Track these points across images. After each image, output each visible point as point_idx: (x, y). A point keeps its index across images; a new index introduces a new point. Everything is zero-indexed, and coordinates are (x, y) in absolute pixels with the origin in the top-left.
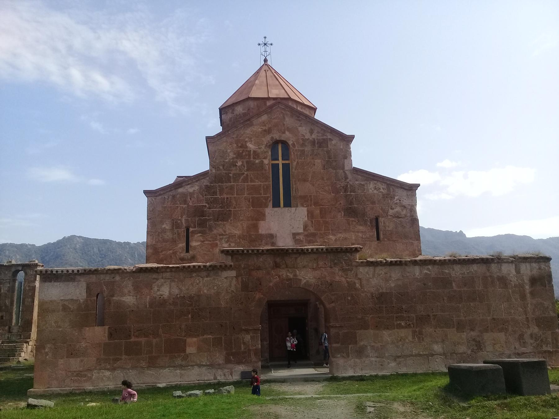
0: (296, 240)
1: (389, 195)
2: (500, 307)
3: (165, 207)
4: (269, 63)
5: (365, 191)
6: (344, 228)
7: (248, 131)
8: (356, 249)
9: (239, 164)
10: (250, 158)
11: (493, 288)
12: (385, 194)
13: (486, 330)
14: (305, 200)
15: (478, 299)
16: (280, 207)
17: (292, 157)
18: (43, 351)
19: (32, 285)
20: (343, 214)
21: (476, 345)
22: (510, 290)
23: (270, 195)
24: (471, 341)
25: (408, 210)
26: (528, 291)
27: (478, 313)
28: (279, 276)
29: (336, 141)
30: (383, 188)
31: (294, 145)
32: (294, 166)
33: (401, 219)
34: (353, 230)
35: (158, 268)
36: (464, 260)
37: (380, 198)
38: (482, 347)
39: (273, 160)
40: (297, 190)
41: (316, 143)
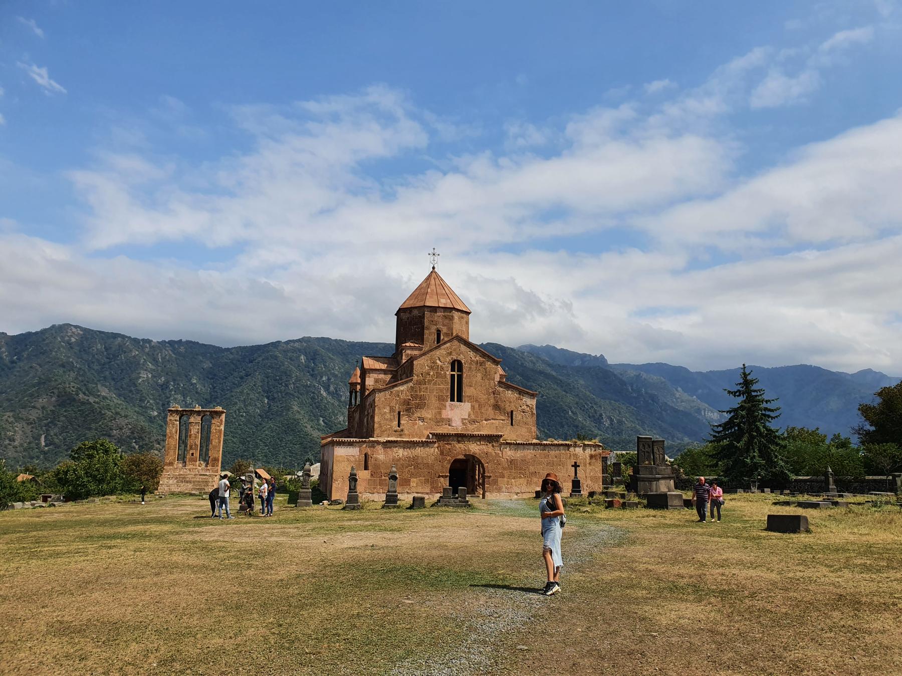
3: (386, 399)
4: (436, 270)
6: (492, 417)
7: (438, 353)
8: (501, 436)
9: (431, 374)
10: (438, 370)
13: (565, 481)
14: (471, 399)
16: (454, 401)
17: (464, 370)
18: (337, 482)
19: (218, 428)
23: (449, 394)
28: (460, 448)
35: (397, 441)
36: (556, 444)
39: (451, 371)
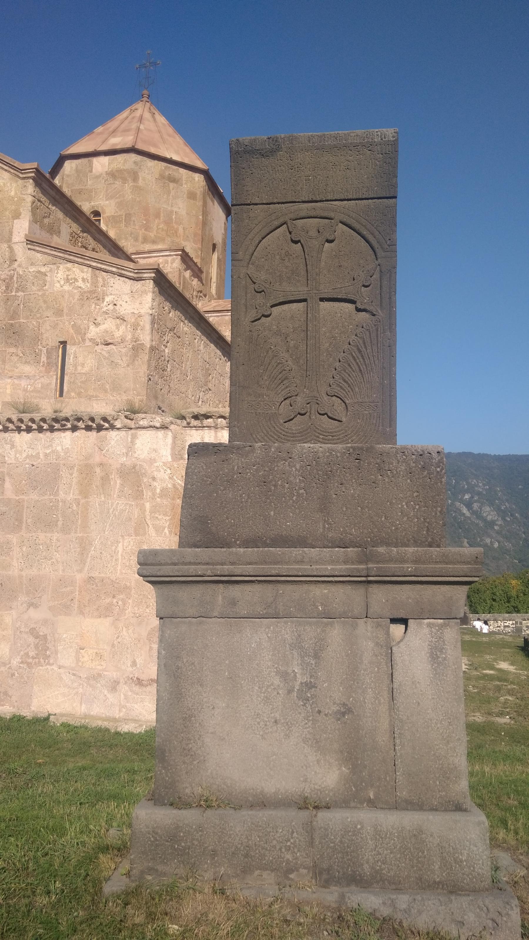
1: (94, 293)
2: (114, 548)
5: (46, 287)
11: (102, 496)
12: (85, 292)
15: (60, 523)
21: (36, 646)
22: (148, 505)
24: (27, 633)
25: (129, 326)
27: (54, 560)
29: (3, 181)
30: (83, 280)
33: (114, 347)
34: (10, 374)
37: (73, 302)
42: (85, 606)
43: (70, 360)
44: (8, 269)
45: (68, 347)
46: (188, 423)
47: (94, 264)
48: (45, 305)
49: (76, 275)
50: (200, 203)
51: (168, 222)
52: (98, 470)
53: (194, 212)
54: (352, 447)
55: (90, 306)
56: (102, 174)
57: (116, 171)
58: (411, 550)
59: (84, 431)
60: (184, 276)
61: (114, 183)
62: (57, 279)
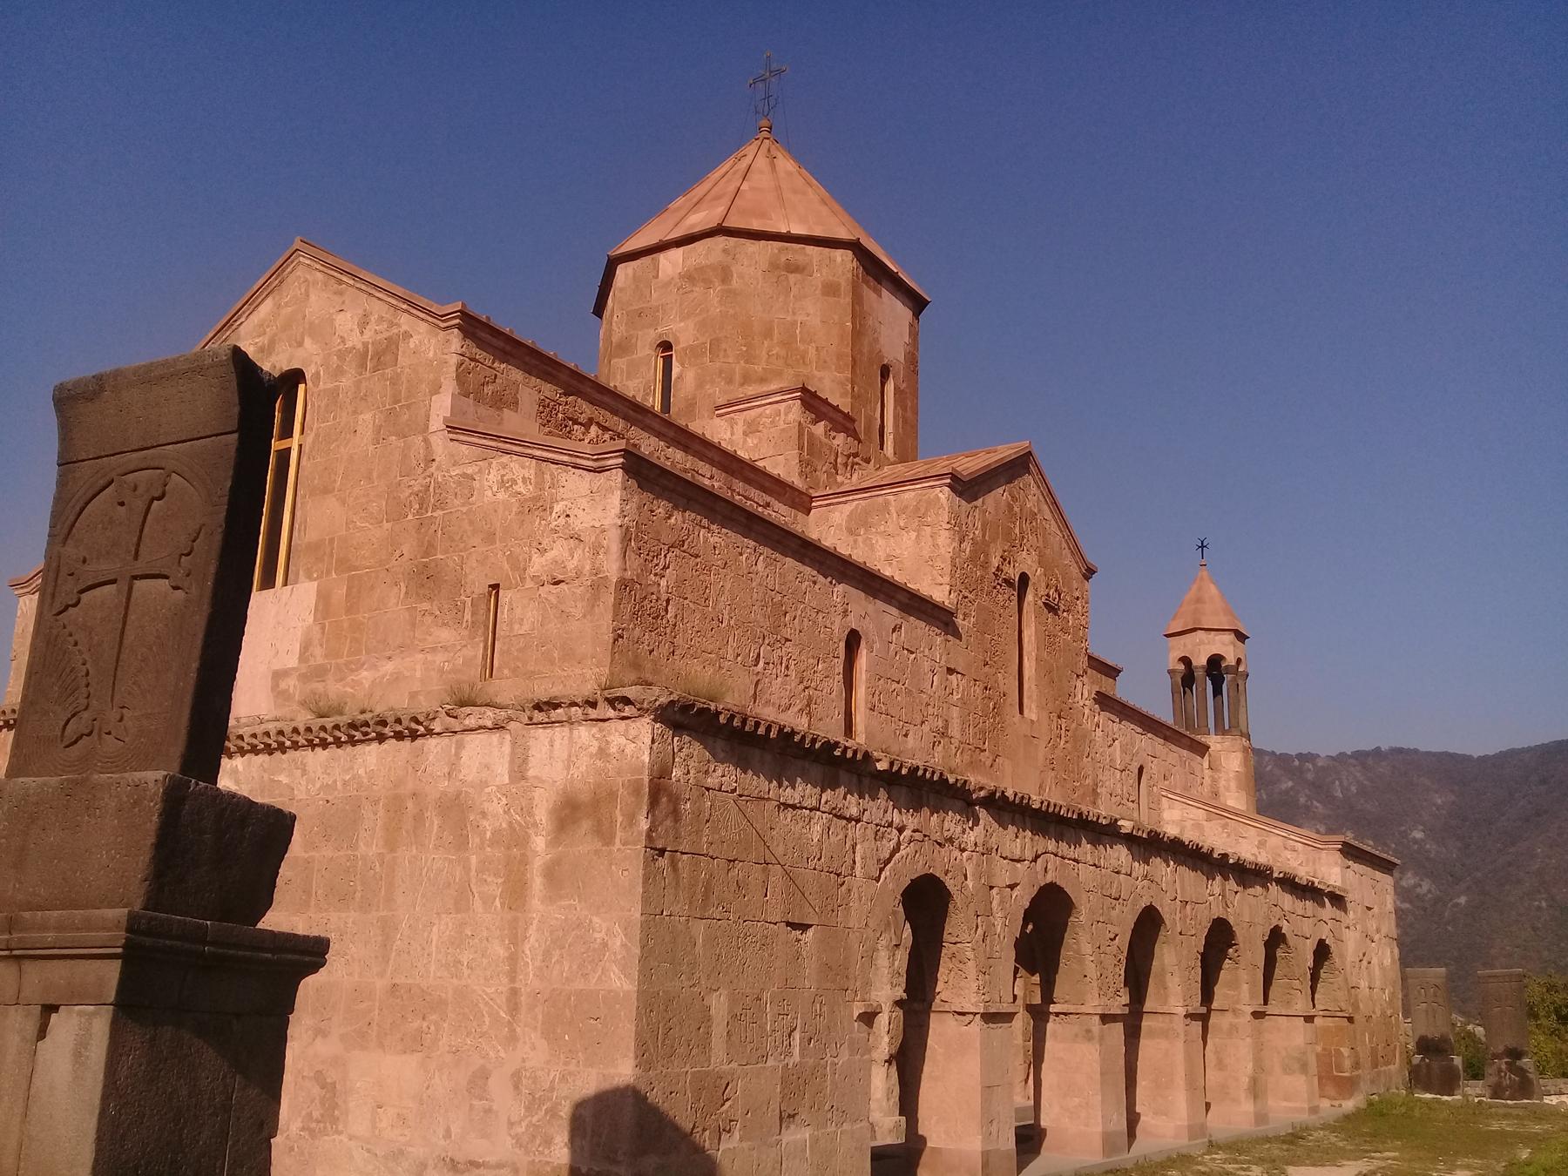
0: (279, 693)
2: (426, 934)
5: (474, 498)
12: (526, 500)
15: (358, 895)
20: (403, 589)
22: (474, 859)
25: (587, 549)
26: (537, 864)
30: (524, 478)
31: (317, 375)
32: (307, 451)
38: (336, 1112)
40: (303, 527)
41: (369, 357)
42: (386, 1034)
43: (503, 615)
44: (423, 476)
45: (501, 592)
46: (530, 718)
47: (538, 453)
48: (471, 528)
49: (514, 474)
50: (846, 300)
51: (787, 343)
52: (410, 804)
53: (836, 317)
54: (66, 780)
55: (532, 523)
56: (672, 278)
57: (696, 269)
58: (56, 913)
59: (394, 741)
60: (811, 435)
61: (692, 291)
62: (488, 483)
